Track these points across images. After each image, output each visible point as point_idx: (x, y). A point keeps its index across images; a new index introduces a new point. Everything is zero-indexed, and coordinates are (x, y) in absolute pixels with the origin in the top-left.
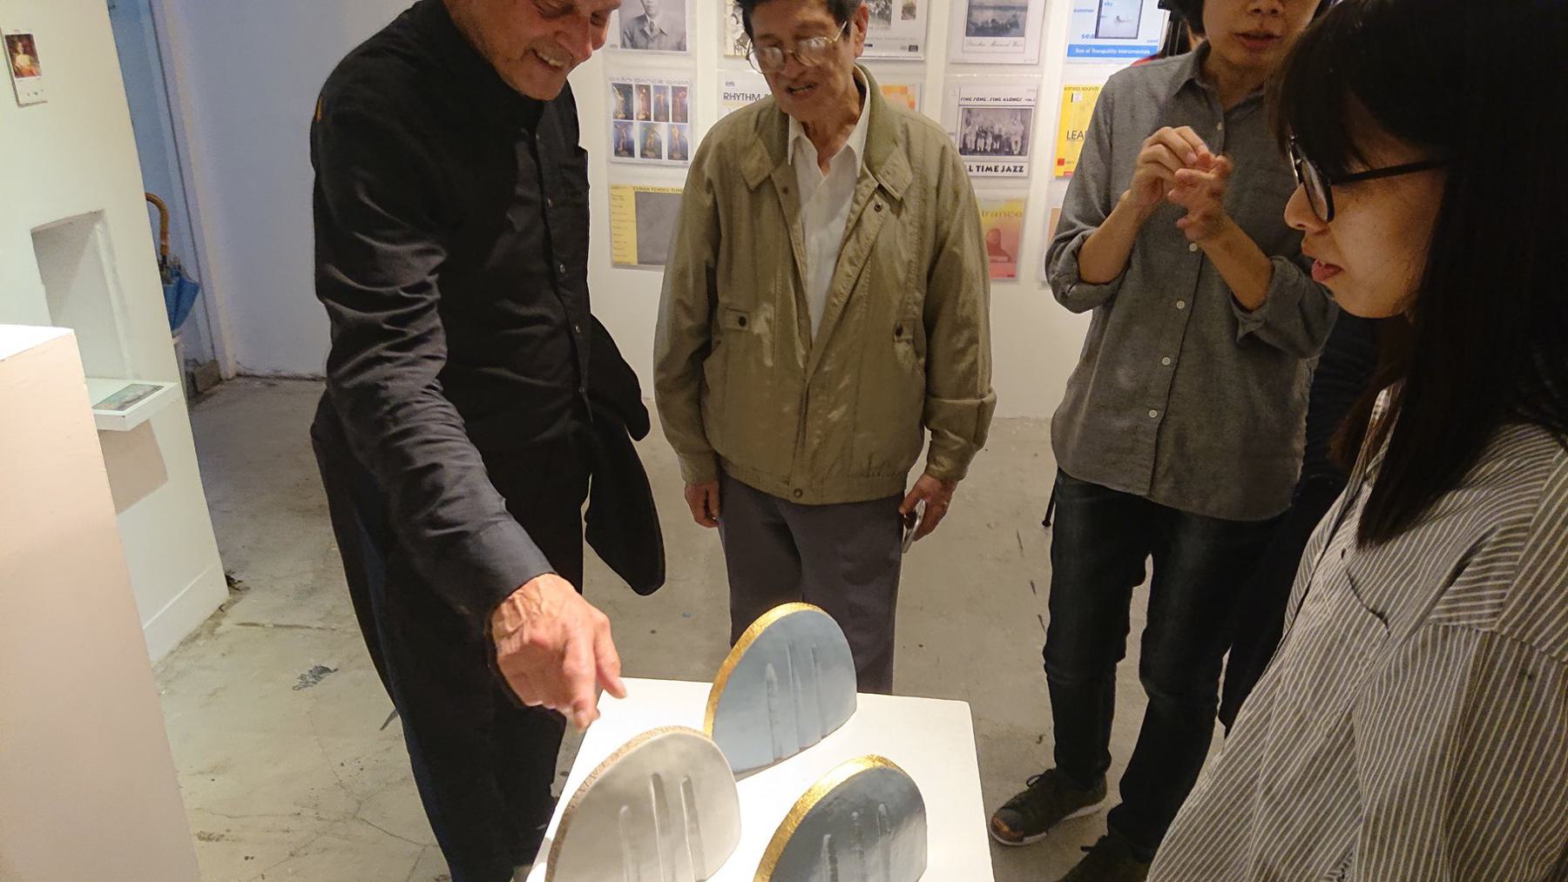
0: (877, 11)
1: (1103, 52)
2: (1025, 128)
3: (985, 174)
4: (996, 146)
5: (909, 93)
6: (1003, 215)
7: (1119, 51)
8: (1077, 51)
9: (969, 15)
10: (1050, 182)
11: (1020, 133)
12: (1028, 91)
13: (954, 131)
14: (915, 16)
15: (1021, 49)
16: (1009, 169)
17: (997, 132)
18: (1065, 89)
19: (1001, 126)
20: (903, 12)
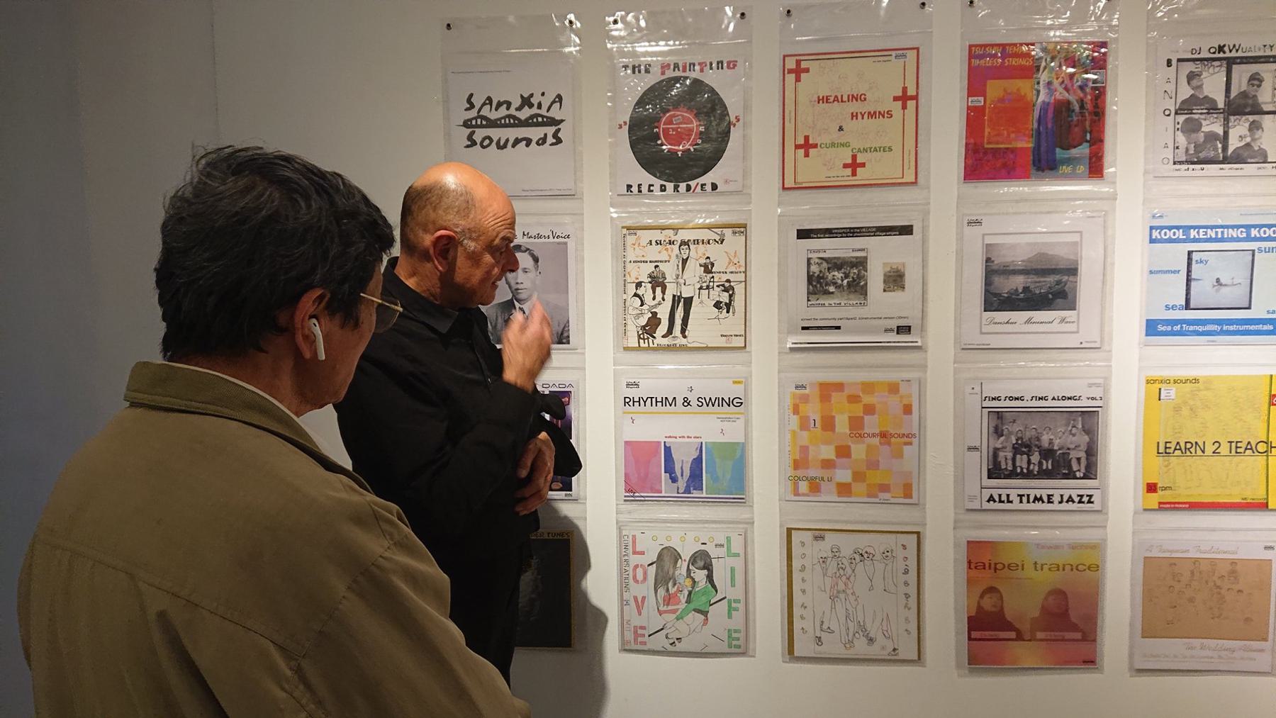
0: (845, 281)
1: (1200, 328)
2: (1090, 438)
3: (1032, 506)
4: (1048, 465)
5: (903, 389)
6: (1068, 568)
7: (1225, 328)
8: (1160, 328)
9: (988, 282)
10: (1135, 513)
11: (1084, 447)
12: (1090, 385)
13: (978, 444)
14: (903, 288)
15: (1073, 327)
16: (1070, 500)
17: (1045, 444)
18: (1148, 382)
19: (1052, 437)
20: (885, 282)
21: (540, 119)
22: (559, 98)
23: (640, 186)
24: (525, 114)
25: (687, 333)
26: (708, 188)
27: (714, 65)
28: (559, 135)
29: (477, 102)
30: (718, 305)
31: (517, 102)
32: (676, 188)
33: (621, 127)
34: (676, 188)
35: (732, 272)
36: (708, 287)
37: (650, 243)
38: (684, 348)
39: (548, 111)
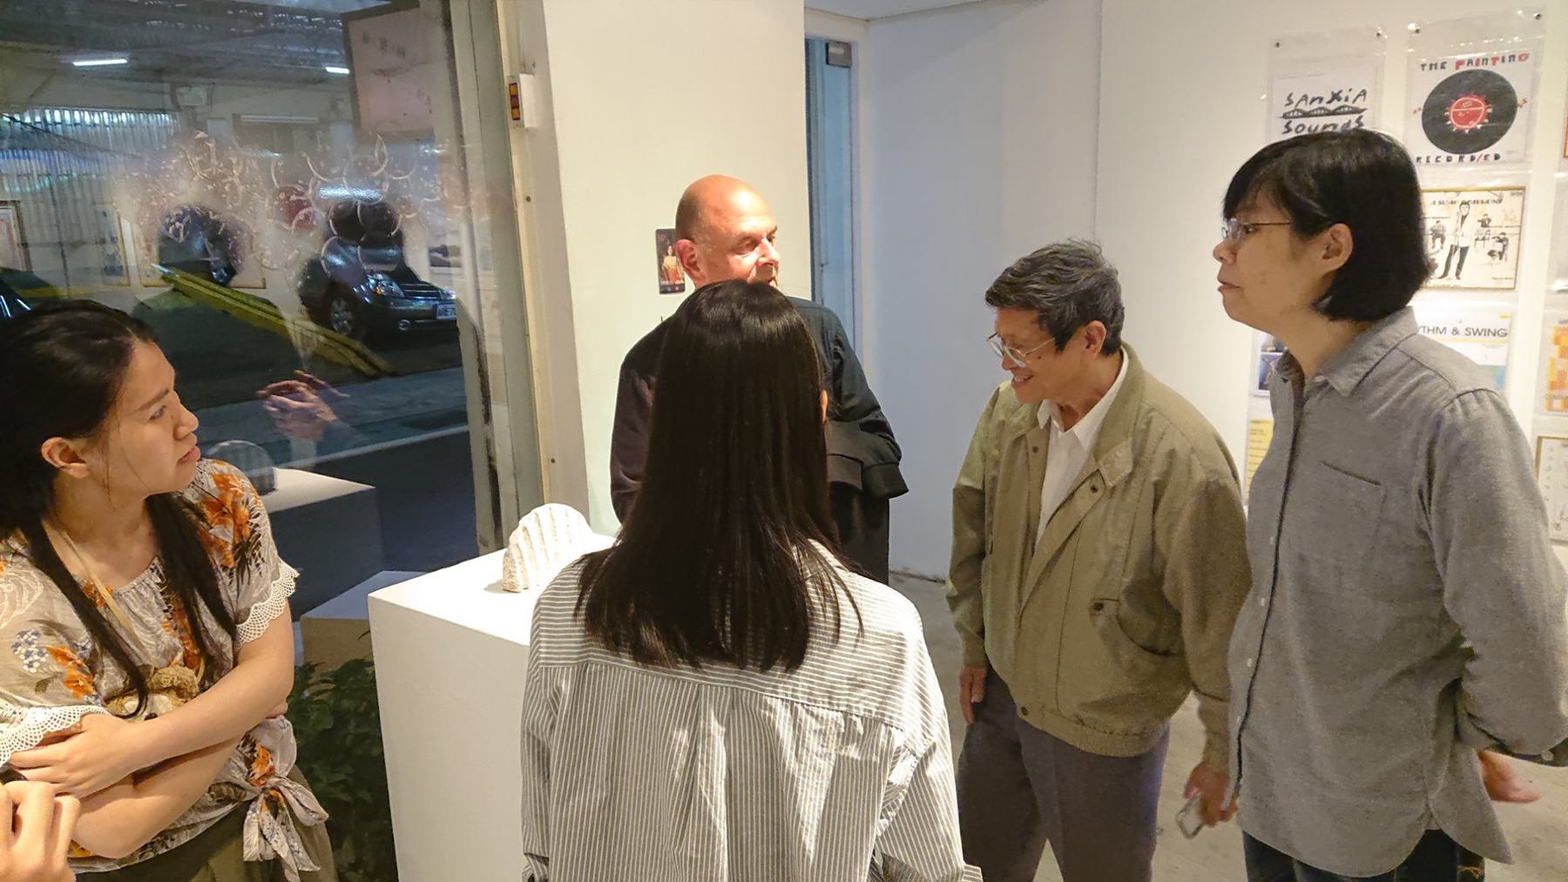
21: (1346, 109)
22: (1364, 93)
23: (1428, 158)
24: (1332, 107)
25: (1460, 276)
26: (1491, 158)
27: (1507, 59)
28: (1362, 120)
29: (1295, 99)
30: (1491, 253)
31: (1328, 97)
32: (1461, 158)
33: (1415, 112)
34: (1461, 158)
35: (1507, 227)
36: (1484, 239)
37: (1434, 203)
38: (1455, 288)
39: (1355, 101)
